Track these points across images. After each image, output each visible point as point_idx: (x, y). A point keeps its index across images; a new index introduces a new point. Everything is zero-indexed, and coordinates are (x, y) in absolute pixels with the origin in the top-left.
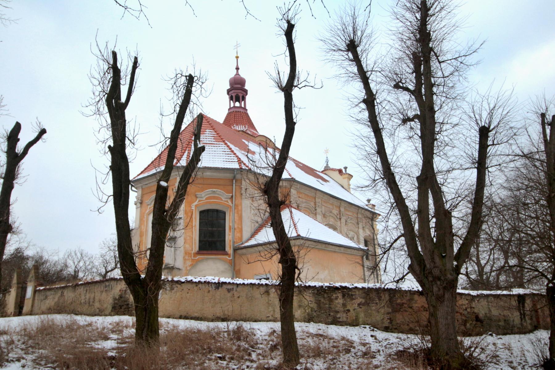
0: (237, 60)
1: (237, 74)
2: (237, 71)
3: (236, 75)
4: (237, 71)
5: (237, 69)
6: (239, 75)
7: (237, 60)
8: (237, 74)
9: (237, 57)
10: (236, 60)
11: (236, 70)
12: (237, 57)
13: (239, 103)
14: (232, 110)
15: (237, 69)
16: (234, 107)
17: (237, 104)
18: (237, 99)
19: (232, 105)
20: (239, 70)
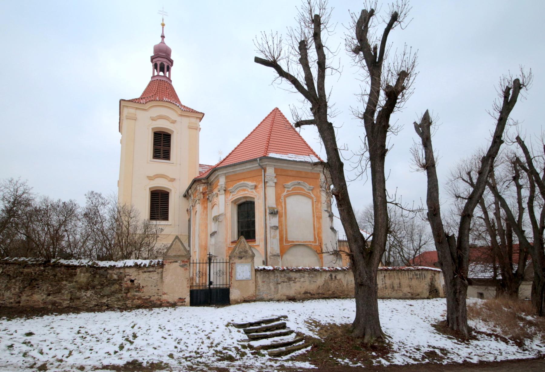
0: (163, 28)
1: (163, 42)
2: (163, 40)
3: (161, 43)
4: (163, 40)
5: (163, 37)
6: (164, 43)
7: (163, 28)
8: (163, 42)
9: (163, 25)
10: (161, 27)
11: (161, 39)
12: (163, 25)
13: (164, 73)
14: (155, 79)
15: (163, 37)
16: (158, 75)
17: (161, 74)
18: (162, 70)
19: (156, 74)
20: (165, 39)
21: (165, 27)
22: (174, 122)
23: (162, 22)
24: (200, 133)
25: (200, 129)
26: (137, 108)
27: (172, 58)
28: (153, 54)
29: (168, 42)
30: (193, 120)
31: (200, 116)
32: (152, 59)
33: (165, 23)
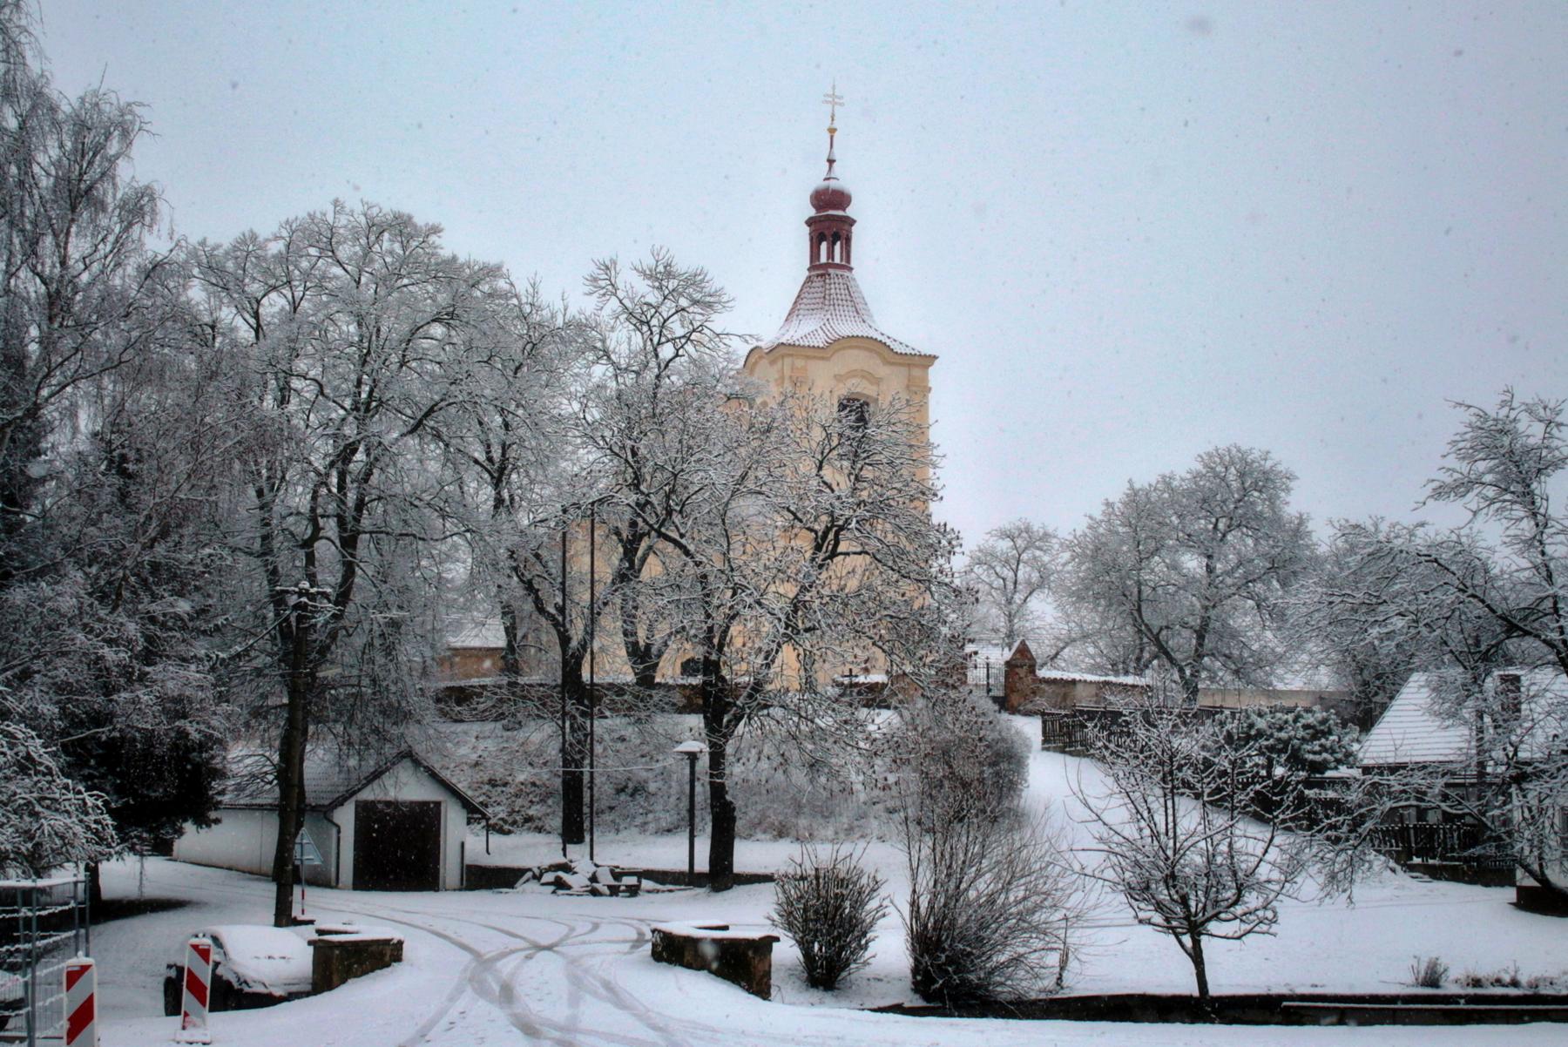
9: (832, 131)
10: (828, 135)
12: (832, 131)
21: (836, 135)
22: (877, 381)
23: (828, 124)
24: (933, 398)
25: (930, 389)
26: (808, 357)
27: (850, 212)
28: (812, 212)
29: (844, 180)
30: (916, 372)
31: (931, 359)
32: (810, 222)
33: (836, 125)
